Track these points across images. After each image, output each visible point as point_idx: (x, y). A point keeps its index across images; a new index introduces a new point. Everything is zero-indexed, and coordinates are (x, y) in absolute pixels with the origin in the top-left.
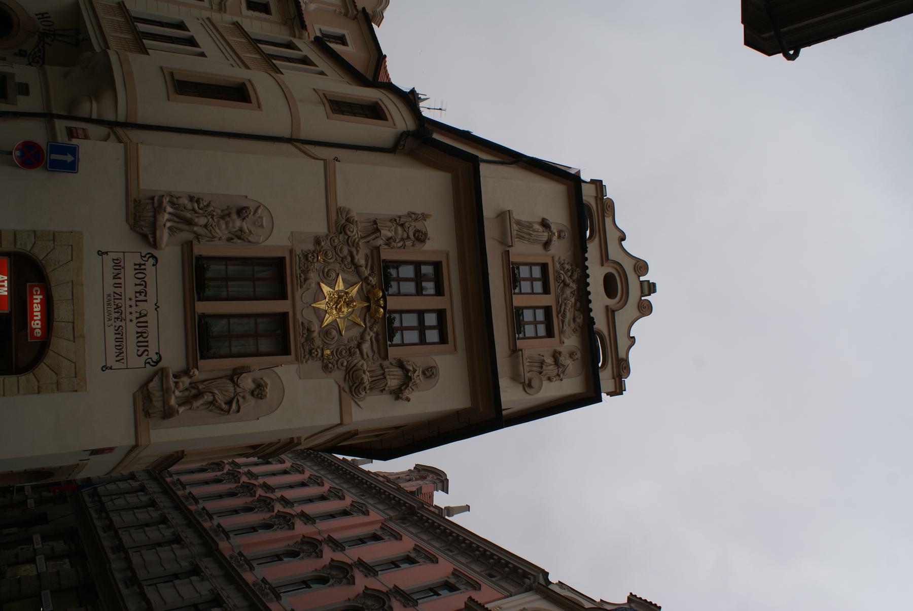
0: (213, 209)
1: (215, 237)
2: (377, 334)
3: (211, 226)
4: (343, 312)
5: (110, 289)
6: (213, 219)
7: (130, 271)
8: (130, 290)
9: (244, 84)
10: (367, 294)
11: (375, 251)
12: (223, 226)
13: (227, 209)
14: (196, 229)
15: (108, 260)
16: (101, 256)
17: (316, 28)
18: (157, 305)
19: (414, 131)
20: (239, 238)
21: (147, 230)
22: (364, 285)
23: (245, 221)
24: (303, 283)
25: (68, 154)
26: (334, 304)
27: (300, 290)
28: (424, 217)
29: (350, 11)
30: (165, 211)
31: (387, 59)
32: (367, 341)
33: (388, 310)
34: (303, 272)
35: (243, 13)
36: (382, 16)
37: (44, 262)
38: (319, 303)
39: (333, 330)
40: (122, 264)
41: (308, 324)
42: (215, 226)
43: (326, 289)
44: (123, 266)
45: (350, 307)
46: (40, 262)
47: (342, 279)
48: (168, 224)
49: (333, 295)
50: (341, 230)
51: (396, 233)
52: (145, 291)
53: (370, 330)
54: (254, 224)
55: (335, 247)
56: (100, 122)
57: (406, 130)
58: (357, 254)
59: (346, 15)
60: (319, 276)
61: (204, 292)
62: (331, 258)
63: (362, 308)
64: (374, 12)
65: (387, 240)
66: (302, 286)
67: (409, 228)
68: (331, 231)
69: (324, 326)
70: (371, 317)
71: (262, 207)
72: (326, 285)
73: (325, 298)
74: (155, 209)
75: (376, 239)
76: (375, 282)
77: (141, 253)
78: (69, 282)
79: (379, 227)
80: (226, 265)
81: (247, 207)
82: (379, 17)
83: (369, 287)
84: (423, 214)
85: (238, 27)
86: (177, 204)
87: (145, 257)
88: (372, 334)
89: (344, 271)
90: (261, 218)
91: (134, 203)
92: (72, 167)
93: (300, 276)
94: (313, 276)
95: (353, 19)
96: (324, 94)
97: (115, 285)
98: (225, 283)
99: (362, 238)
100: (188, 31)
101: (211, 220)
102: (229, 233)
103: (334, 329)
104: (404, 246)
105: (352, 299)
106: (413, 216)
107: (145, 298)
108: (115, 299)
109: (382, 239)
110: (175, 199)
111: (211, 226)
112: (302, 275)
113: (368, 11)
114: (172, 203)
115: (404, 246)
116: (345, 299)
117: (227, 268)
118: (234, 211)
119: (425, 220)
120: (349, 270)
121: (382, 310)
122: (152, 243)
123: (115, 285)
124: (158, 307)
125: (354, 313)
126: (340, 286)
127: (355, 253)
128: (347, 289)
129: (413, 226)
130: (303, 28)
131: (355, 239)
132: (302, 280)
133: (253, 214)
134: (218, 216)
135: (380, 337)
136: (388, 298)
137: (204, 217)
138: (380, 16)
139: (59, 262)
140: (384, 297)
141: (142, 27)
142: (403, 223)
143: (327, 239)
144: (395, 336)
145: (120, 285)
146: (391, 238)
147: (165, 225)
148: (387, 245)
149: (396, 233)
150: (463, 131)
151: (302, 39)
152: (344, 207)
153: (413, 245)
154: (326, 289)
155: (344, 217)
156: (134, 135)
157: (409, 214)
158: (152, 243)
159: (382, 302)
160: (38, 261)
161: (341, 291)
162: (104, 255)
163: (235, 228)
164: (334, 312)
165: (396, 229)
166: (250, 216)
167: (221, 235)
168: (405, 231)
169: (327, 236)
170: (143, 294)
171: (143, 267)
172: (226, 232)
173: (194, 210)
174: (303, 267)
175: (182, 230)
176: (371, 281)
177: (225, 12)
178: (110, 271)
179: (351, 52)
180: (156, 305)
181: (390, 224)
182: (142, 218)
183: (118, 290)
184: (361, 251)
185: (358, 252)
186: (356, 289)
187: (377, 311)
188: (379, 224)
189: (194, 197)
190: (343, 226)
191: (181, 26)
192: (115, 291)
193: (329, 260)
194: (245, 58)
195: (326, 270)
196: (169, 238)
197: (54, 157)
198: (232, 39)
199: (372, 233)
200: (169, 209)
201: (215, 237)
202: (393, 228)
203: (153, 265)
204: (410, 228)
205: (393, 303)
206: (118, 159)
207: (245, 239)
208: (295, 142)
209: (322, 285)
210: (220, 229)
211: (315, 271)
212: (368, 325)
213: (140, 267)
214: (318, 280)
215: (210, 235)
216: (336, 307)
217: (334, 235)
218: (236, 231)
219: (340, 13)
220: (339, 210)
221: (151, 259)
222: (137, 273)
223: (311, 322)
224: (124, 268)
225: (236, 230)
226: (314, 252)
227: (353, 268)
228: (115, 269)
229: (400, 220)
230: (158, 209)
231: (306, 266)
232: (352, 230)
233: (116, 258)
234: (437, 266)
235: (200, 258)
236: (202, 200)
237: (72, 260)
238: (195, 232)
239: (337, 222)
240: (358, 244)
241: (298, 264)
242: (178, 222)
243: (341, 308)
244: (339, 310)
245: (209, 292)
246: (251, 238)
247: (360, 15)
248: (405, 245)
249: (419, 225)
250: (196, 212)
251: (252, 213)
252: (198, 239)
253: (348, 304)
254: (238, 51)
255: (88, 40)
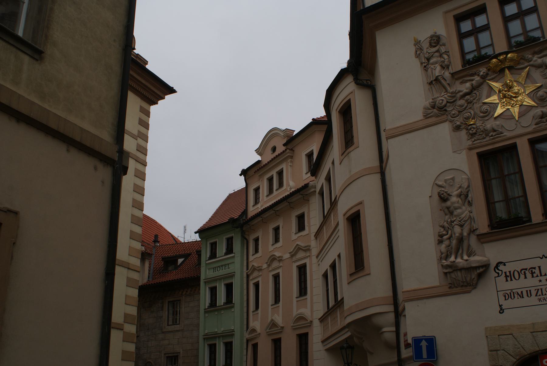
0: (446, 222)
1: (470, 216)
2: (534, 53)
3: (460, 221)
4: (519, 90)
5: (534, 300)
6: (454, 221)
7: (513, 285)
8: (531, 282)
9: (348, 219)
10: (497, 73)
11: (456, 77)
12: (459, 211)
13: (444, 211)
14: (465, 234)
15: (506, 304)
16: (504, 310)
17: (305, 177)
18: (541, 257)
19: (353, 75)
20: (467, 196)
21: (474, 275)
22: (489, 78)
23: (451, 194)
24: (497, 132)
25: (421, 345)
26: (513, 100)
27: (504, 134)
28: (417, 43)
29: (288, 154)
30: (454, 262)
31: (315, 118)
32: (542, 61)
33: (508, 49)
34: (487, 135)
35: (308, 233)
36: (286, 130)
37: (518, 358)
38: (514, 114)
39: (538, 95)
40: (508, 292)
41: (536, 119)
42: (461, 217)
43: (499, 111)
44: (510, 291)
45: (512, 85)
46: (518, 360)
47: (487, 99)
48: (465, 257)
49: (504, 103)
50: (443, 111)
51: (436, 63)
52: (529, 270)
53: (531, 61)
54: (452, 185)
55: (459, 112)
56: (397, 325)
57: (354, 82)
58: (462, 91)
59: (292, 157)
60: (488, 120)
61: (522, 217)
62: (470, 113)
63: (511, 74)
64: (284, 137)
65: (444, 68)
66: (501, 132)
67: (429, 53)
68: (446, 119)
69: (535, 104)
70: (519, 64)
71: (435, 183)
72: (495, 112)
73: (508, 109)
74: (454, 270)
75: (445, 77)
76: (484, 69)
77: (495, 277)
78: (533, 336)
79: (434, 79)
80: (494, 203)
81: (438, 194)
82: (287, 132)
83: (490, 73)
84: (415, 45)
85: (318, 234)
86: (447, 253)
87: (498, 273)
88: (535, 59)
89: (479, 99)
90: (446, 181)
91: (453, 288)
92: (431, 341)
93: (492, 136)
94: (490, 124)
95: (294, 151)
96: (342, 155)
97: (529, 295)
98: (512, 201)
99: (446, 91)
100: (327, 270)
101: (455, 223)
102: (464, 205)
103: (537, 94)
104: (446, 52)
105: (505, 85)
106: (418, 53)
107: (537, 269)
108: (542, 295)
109: (444, 73)
110: (443, 255)
111: (460, 221)
112: (490, 135)
113: (285, 141)
114: (447, 257)
115: (446, 52)
116: (506, 91)
117: (497, 202)
118: (444, 205)
119: (420, 41)
120: (478, 95)
121: (509, 55)
122: (484, 268)
123: (529, 295)
124: (543, 255)
125: (518, 80)
126: (494, 99)
127: (461, 93)
128: (496, 92)
129: (428, 50)
130: (308, 186)
131: (448, 96)
132: (494, 133)
133: (444, 188)
134: (451, 217)
135: (537, 49)
136: (497, 53)
137: (454, 229)
138: (286, 131)
139: (516, 345)
140: (496, 56)
141: (332, 303)
142: (426, 59)
143: (454, 120)
144: (533, 36)
145: (529, 292)
146: (441, 66)
147: (466, 260)
148: (448, 68)
149: (436, 63)
150: (350, 39)
151: (316, 186)
152: (423, 113)
153: (444, 45)
154: (499, 111)
155: (430, 111)
156: (401, 297)
157: (417, 56)
158: (484, 268)
159: (501, 57)
160: (517, 362)
161: (499, 96)
162: (503, 308)
163: (458, 200)
164: (520, 98)
165: (432, 64)
166: (446, 190)
167: (467, 212)
168: (432, 56)
169: (450, 122)
170: (534, 270)
171: (508, 274)
172: (464, 208)
173: (449, 238)
174: (483, 135)
175: (469, 246)
176: (484, 73)
177: (310, 246)
178: (517, 301)
179: (315, 147)
180: (541, 258)
181: (429, 70)
182: (464, 280)
183: (534, 293)
184: (459, 89)
185: (460, 92)
186: (494, 84)
187: (511, 60)
188: (432, 79)
189: (438, 240)
190: (439, 109)
191: (325, 276)
192: (535, 295)
193: (472, 114)
194: (335, 224)
195: (482, 115)
196: (478, 256)
197: (425, 355)
198: (325, 238)
199: (440, 82)
200: (452, 259)
201: (470, 216)
202: (432, 66)
203: (505, 265)
204: (429, 52)
205: (501, 46)
206: (418, 306)
207: (467, 190)
208: (383, 169)
209: (496, 115)
210: (463, 213)
211: (484, 124)
212: (526, 64)
213: (508, 276)
214: (492, 119)
215: (469, 221)
216: (515, 97)
217: (449, 115)
218: (461, 199)
219: (291, 162)
220: (426, 116)
221: (499, 268)
222: (515, 279)
223: (533, 117)
224: (511, 290)
225: (460, 200)
226: (467, 129)
227: (475, 92)
228: (514, 297)
229: (424, 63)
230: (453, 268)
231: (481, 133)
232: (441, 101)
233: (504, 297)
234: (459, 19)
235: (491, 226)
236: (439, 232)
237: (512, 334)
238: (469, 234)
239: (437, 116)
240: (452, 93)
241: (480, 141)
242: (463, 250)
243: (515, 93)
244: (517, 94)
245: (523, 214)
246: (465, 185)
247: (289, 146)
248: (445, 52)
249: (425, 45)
250: (451, 236)
251: (443, 189)
252: (474, 230)
253: (510, 88)
254: (332, 230)
255: (346, 340)
